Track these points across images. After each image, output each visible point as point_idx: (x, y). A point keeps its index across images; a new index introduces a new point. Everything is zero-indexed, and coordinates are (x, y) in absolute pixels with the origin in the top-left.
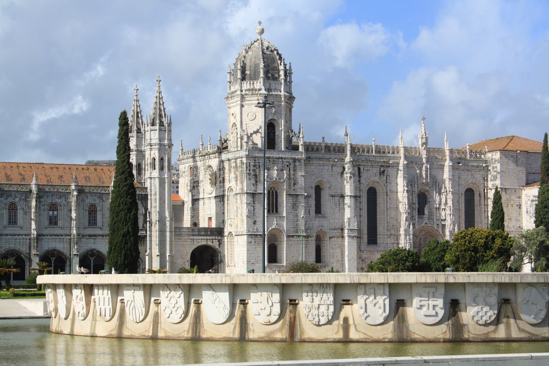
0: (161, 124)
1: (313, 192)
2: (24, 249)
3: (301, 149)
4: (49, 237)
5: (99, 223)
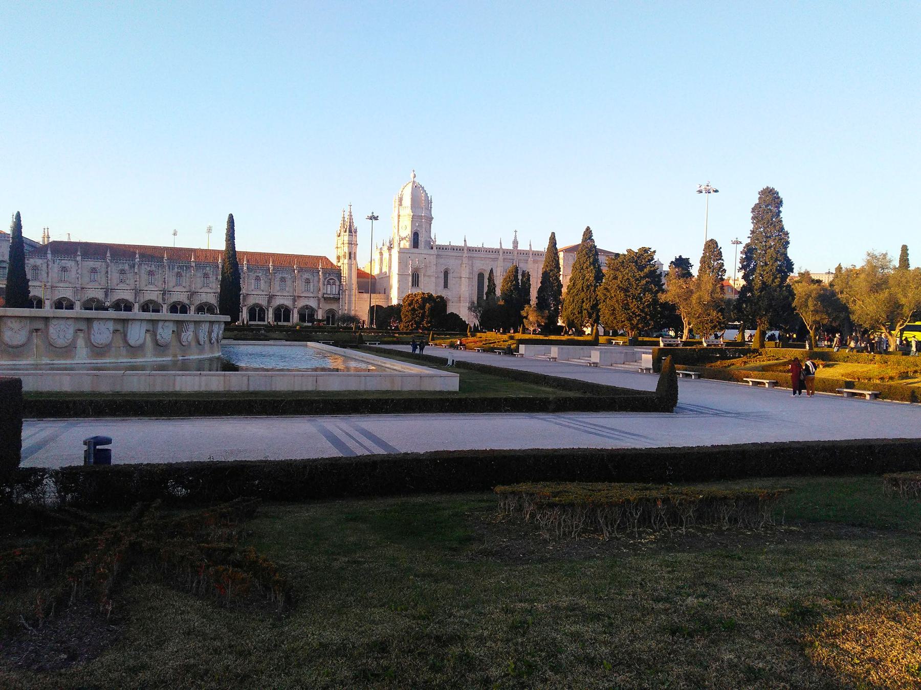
0: (350, 231)
1: (442, 275)
2: (265, 304)
3: (434, 248)
4: (280, 297)
5: (312, 290)
